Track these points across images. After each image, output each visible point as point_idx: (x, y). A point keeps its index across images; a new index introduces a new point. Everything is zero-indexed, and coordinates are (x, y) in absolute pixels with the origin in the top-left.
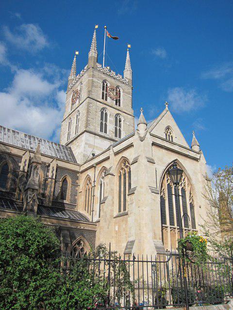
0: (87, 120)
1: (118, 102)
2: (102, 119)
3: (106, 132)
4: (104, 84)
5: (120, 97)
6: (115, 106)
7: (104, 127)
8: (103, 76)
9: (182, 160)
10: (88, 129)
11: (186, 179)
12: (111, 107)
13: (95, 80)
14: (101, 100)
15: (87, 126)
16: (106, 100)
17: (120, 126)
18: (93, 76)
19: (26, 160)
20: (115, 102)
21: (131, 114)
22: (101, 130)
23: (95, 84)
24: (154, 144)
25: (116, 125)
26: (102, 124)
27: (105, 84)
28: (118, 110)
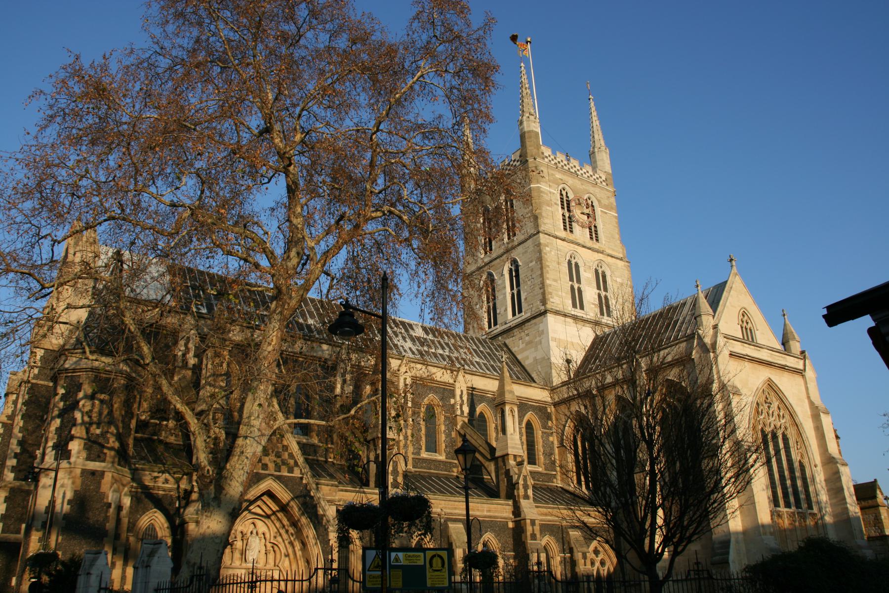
1: (594, 233)
2: (571, 279)
3: (582, 308)
4: (561, 194)
6: (589, 243)
7: (577, 298)
8: (558, 176)
12: (584, 247)
16: (571, 231)
19: (462, 391)
20: (588, 230)
21: (621, 256)
24: (732, 355)
25: (599, 288)
26: (572, 288)
27: (564, 193)
28: (598, 251)
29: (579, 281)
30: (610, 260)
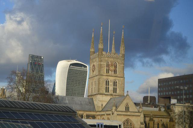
0: (99, 88)
2: (106, 85)
3: (108, 92)
5: (116, 68)
7: (107, 90)
9: (130, 118)
10: (99, 93)
11: (132, 125)
13: (102, 63)
14: (106, 74)
15: (98, 92)
16: (109, 73)
17: (116, 86)
18: (101, 61)
22: (106, 92)
23: (102, 66)
25: (114, 86)
26: (106, 87)
29: (108, 85)
30: (119, 78)
